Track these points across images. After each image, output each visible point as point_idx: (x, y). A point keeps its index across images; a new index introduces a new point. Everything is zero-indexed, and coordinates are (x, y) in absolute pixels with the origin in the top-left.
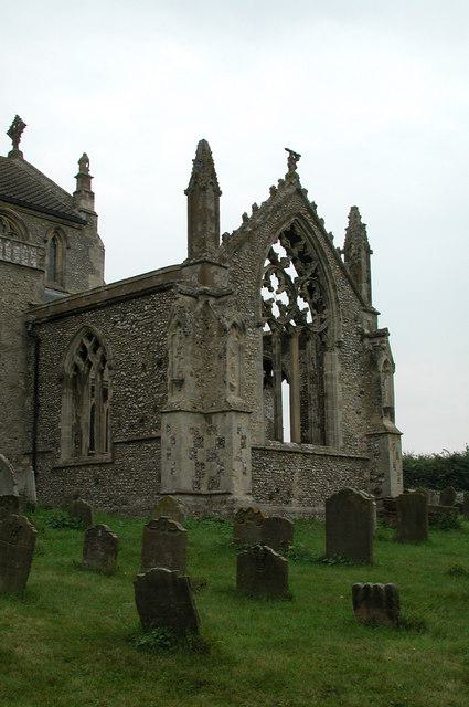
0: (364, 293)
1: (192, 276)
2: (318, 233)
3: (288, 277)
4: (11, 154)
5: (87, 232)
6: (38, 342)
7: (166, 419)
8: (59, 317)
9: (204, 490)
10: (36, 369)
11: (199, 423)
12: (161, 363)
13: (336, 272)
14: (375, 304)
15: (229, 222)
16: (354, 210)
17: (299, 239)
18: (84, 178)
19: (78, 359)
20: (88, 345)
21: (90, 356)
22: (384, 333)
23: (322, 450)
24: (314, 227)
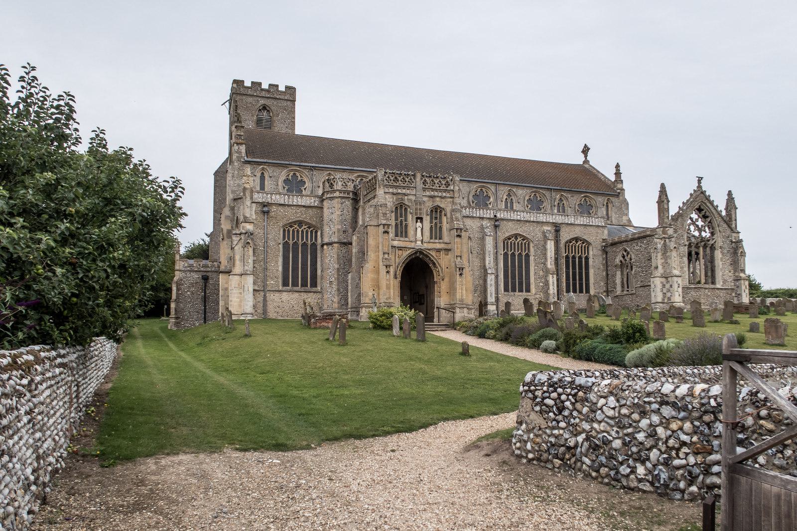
0: (733, 226)
1: (660, 231)
2: (711, 207)
3: (697, 226)
4: (584, 162)
5: (621, 198)
6: (607, 253)
7: (652, 280)
8: (614, 244)
9: (666, 301)
10: (607, 262)
11: (664, 280)
12: (650, 259)
13: (720, 219)
14: (739, 229)
15: (673, 210)
16: (730, 192)
17: (703, 210)
18: (618, 174)
19: (622, 259)
20: (625, 254)
21: (626, 258)
22: (741, 241)
23: (713, 286)
24: (708, 204)
